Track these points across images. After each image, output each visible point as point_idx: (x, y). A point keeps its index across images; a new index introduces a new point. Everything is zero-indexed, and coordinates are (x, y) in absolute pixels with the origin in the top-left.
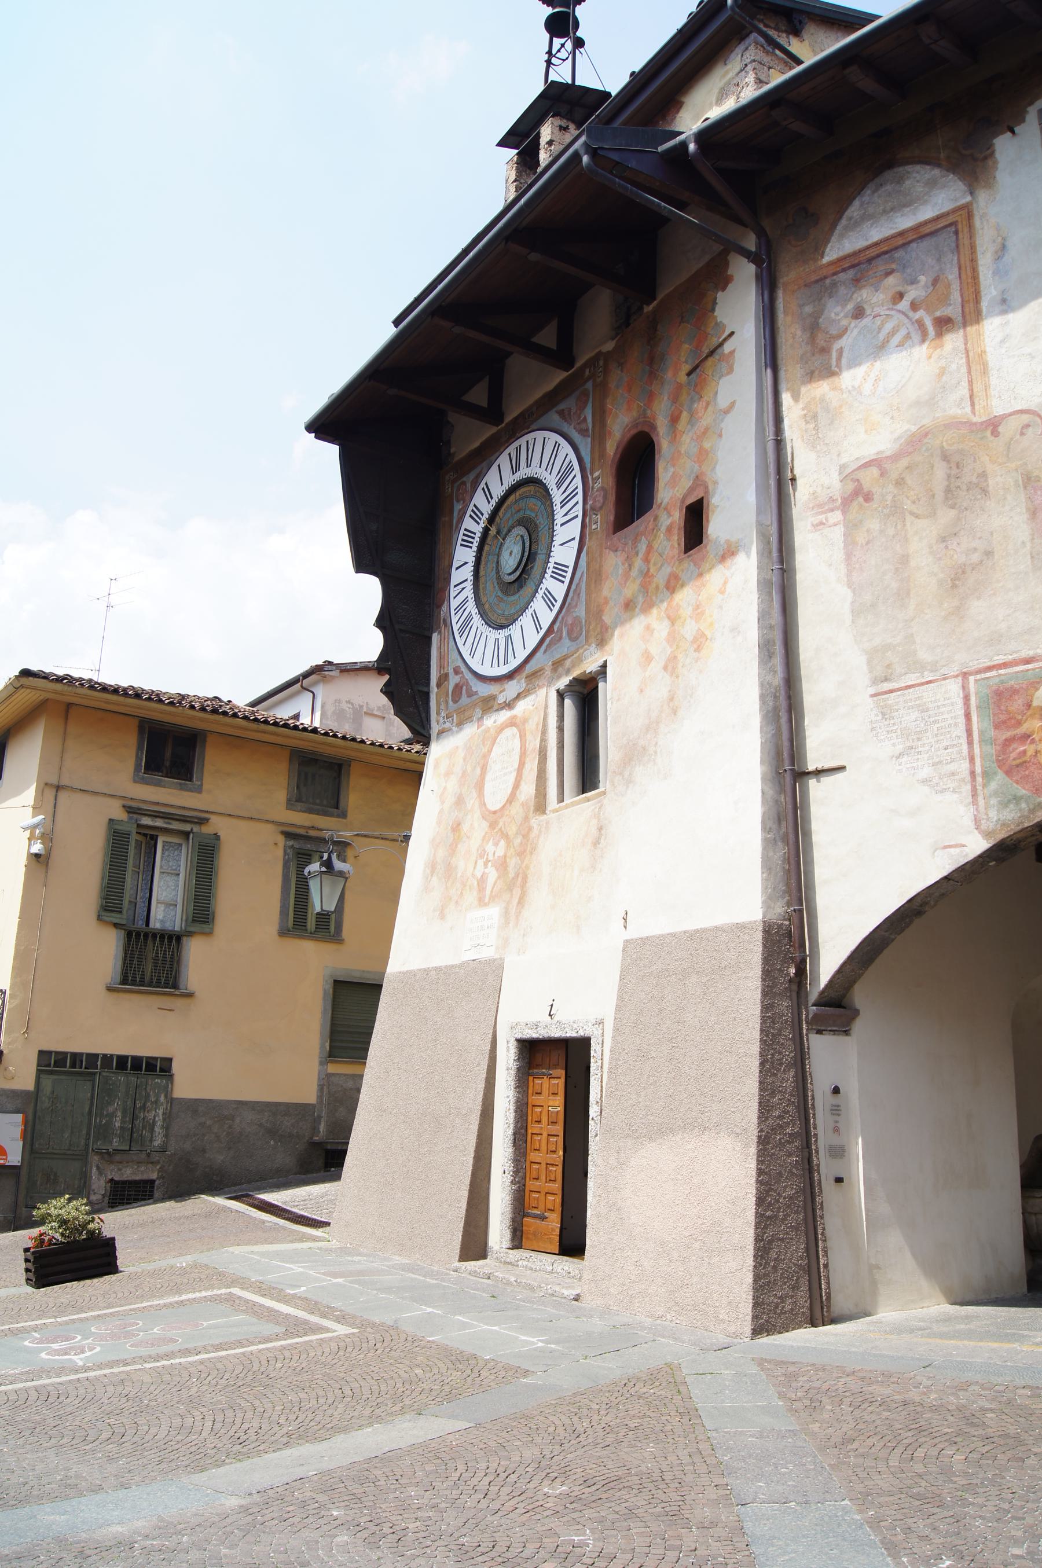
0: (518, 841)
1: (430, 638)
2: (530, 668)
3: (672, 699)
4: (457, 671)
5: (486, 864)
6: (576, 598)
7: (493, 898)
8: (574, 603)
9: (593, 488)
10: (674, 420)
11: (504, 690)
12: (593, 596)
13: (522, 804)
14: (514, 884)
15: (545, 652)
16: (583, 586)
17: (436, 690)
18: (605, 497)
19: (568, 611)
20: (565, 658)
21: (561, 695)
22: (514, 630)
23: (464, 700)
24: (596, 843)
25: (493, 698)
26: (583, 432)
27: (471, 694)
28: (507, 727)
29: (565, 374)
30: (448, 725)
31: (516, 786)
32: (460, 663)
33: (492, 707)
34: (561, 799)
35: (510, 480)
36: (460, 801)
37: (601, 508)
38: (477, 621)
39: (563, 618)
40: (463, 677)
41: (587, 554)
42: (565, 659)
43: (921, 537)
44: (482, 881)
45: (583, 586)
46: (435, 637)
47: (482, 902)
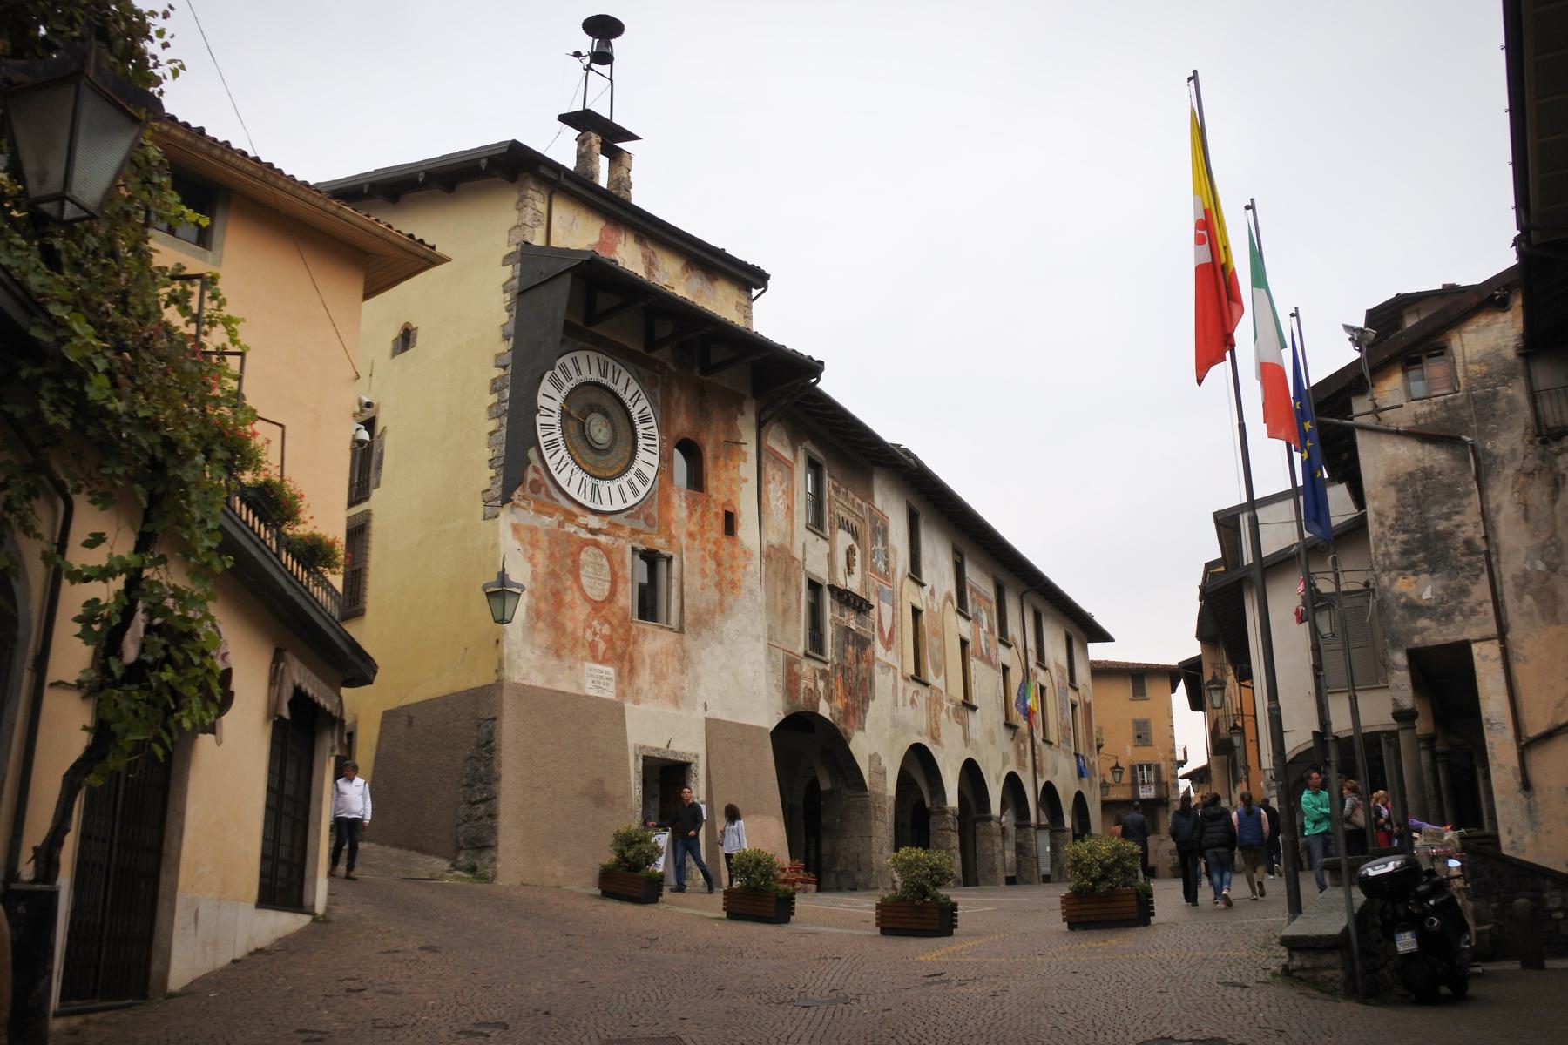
0: (621, 631)
2: (611, 518)
3: (721, 604)
4: (536, 470)
5: (595, 634)
7: (604, 661)
10: (716, 457)
14: (623, 659)
22: (603, 486)
23: (542, 496)
24: (681, 659)
29: (641, 350)
30: (523, 503)
32: (539, 465)
36: (553, 574)
43: (780, 588)
44: (593, 646)
47: (595, 659)
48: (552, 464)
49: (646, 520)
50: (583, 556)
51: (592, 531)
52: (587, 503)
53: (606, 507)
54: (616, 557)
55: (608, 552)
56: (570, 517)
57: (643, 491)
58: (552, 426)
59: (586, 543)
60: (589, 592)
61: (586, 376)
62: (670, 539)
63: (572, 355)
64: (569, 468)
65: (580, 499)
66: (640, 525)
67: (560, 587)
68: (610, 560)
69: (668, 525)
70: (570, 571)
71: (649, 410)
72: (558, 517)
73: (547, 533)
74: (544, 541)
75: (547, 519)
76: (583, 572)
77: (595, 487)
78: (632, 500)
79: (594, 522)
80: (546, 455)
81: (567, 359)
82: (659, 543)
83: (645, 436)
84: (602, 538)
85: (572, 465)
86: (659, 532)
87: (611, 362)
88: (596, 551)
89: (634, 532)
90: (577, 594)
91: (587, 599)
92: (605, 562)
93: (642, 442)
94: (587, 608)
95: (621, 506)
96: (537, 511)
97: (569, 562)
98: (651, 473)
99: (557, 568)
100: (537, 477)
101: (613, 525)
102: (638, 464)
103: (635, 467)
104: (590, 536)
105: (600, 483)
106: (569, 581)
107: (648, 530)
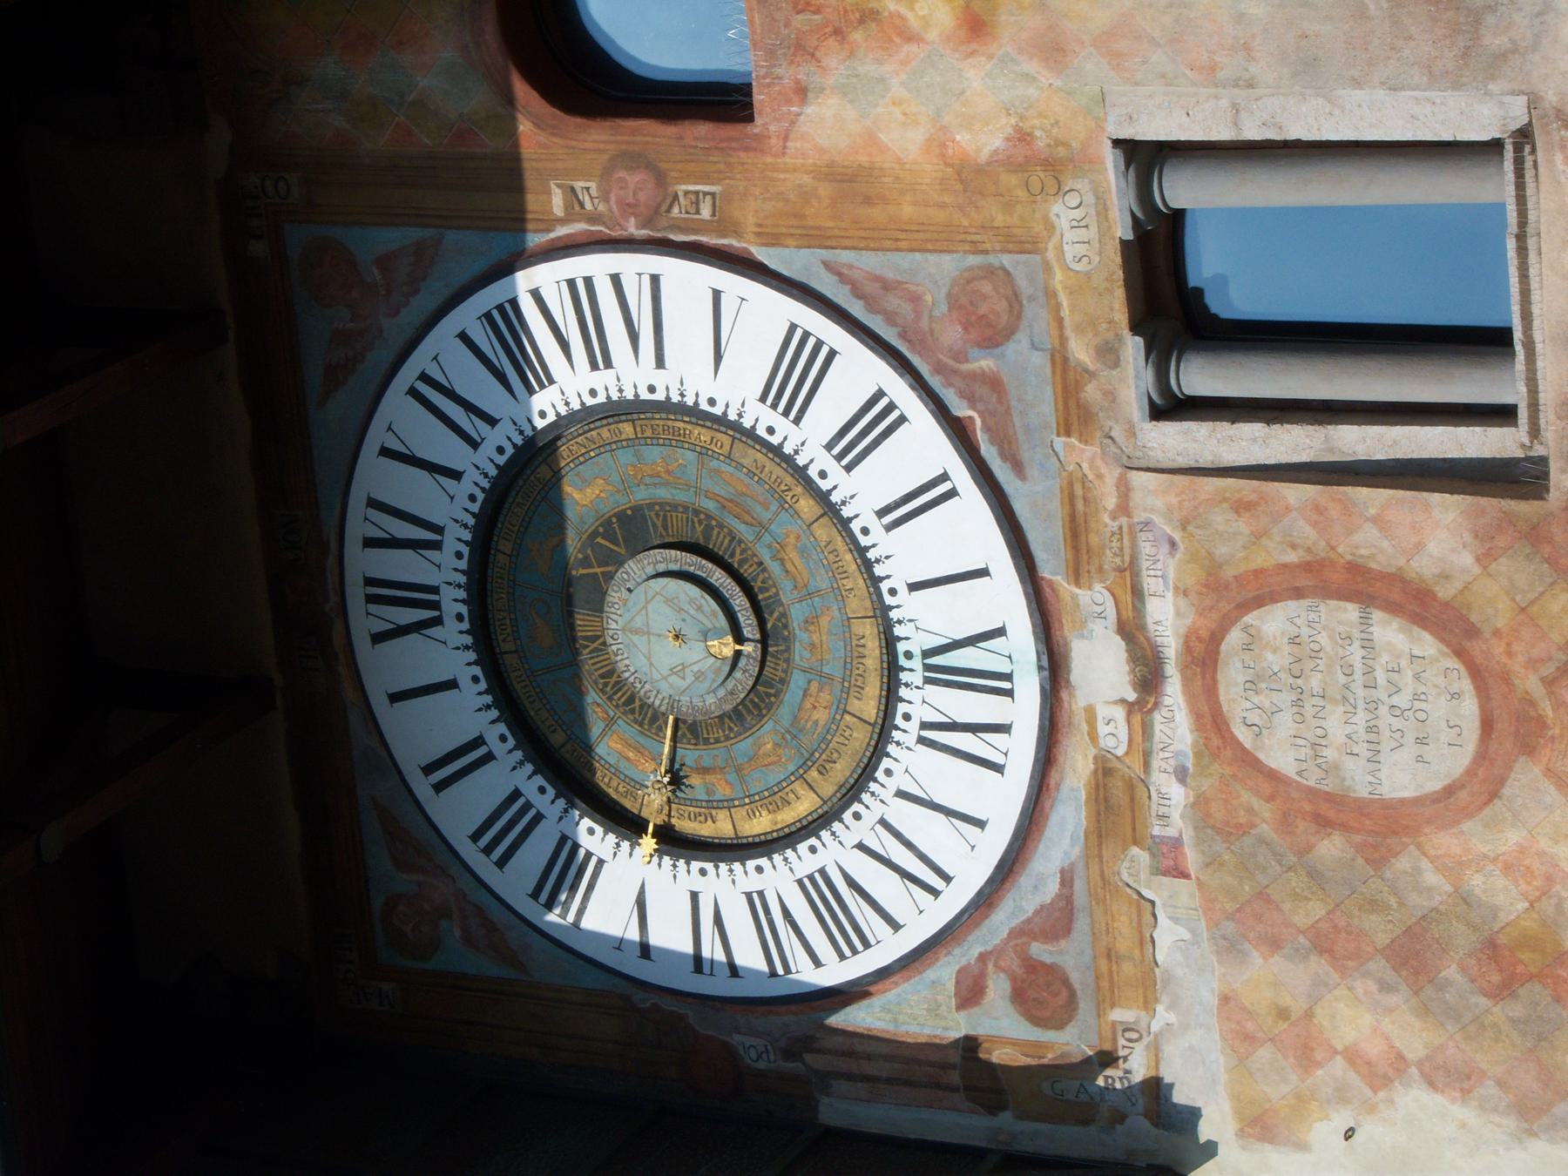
1: (830, 1133)
6: (893, 302)
8: (906, 309)
9: (593, 218)
11: (1090, 712)
12: (907, 210)
13: (1485, 559)
15: (1018, 467)
16: (867, 262)
17: (1005, 1119)
18: (633, 160)
19: (920, 345)
20: (1060, 360)
21: (1172, 407)
22: (924, 621)
23: (1070, 956)
25: (1105, 770)
26: (423, 258)
27: (1057, 920)
28: (1211, 691)
31: (1415, 602)
32: (945, 971)
33: (1131, 787)
34: (1502, 414)
35: (448, 652)
36: (1413, 957)
37: (661, 179)
38: (832, 852)
39: (939, 369)
40: (998, 952)
41: (774, 240)
42: (1065, 360)
45: (867, 262)
46: (836, 1110)
48: (924, 918)
49: (993, 336)
50: (1281, 757)
51: (1149, 678)
52: (1025, 710)
53: (1003, 598)
54: (1233, 540)
55: (1230, 596)
56: (1117, 805)
57: (858, 373)
58: (756, 902)
59: (1211, 720)
60: (1451, 758)
61: (467, 712)
62: (1041, 164)
63: (422, 787)
64: (908, 818)
65: (1021, 750)
66: (1023, 363)
67: (1463, 939)
68: (1261, 591)
69: (970, 178)
70: (1377, 857)
71: (467, 316)
72: (1135, 865)
73: (1230, 949)
74: (1271, 977)
75: (1168, 936)
76: (1359, 780)
77: (940, 676)
78: (922, 448)
79: (1100, 668)
80: (888, 949)
81: (458, 812)
82: (1084, 233)
83: (600, 358)
84: (1166, 619)
85: (880, 801)
86: (1027, 245)
87: (361, 563)
88: (1232, 676)
89: (1076, 416)
90: (1481, 838)
91: (1481, 787)
92: (1275, 621)
93: (631, 376)
94: (1525, 779)
95: (972, 503)
96: (1148, 987)
97: (1331, 848)
98: (763, 315)
99: (1380, 930)
100: (998, 987)
101: (1076, 530)
102: (737, 390)
103: (760, 417)
104: (1173, 689)
105: (912, 641)
106: (1423, 874)
107: (1036, 319)
